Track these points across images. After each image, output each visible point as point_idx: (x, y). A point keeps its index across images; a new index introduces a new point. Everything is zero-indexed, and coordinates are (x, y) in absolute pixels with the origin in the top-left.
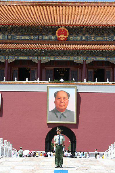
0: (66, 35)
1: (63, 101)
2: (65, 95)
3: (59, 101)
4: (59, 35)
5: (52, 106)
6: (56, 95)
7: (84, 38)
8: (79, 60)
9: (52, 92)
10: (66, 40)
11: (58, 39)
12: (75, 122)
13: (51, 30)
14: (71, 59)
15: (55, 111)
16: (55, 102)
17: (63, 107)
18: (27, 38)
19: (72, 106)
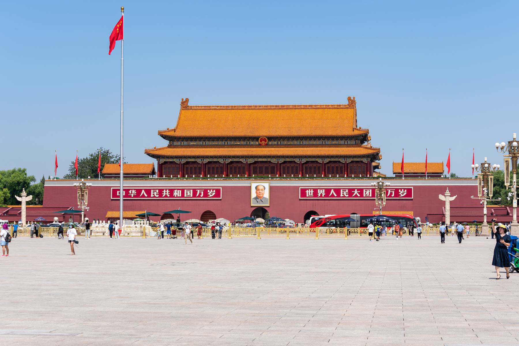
0: (265, 141)
1: (261, 192)
2: (262, 188)
3: (258, 192)
4: (261, 141)
5: (254, 195)
6: (256, 188)
7: (279, 143)
8: (274, 161)
9: (254, 185)
10: (266, 145)
11: (260, 145)
12: (268, 205)
13: (256, 138)
14: (269, 160)
15: (256, 198)
16: (256, 193)
17: (261, 196)
18: (238, 143)
19: (266, 195)
